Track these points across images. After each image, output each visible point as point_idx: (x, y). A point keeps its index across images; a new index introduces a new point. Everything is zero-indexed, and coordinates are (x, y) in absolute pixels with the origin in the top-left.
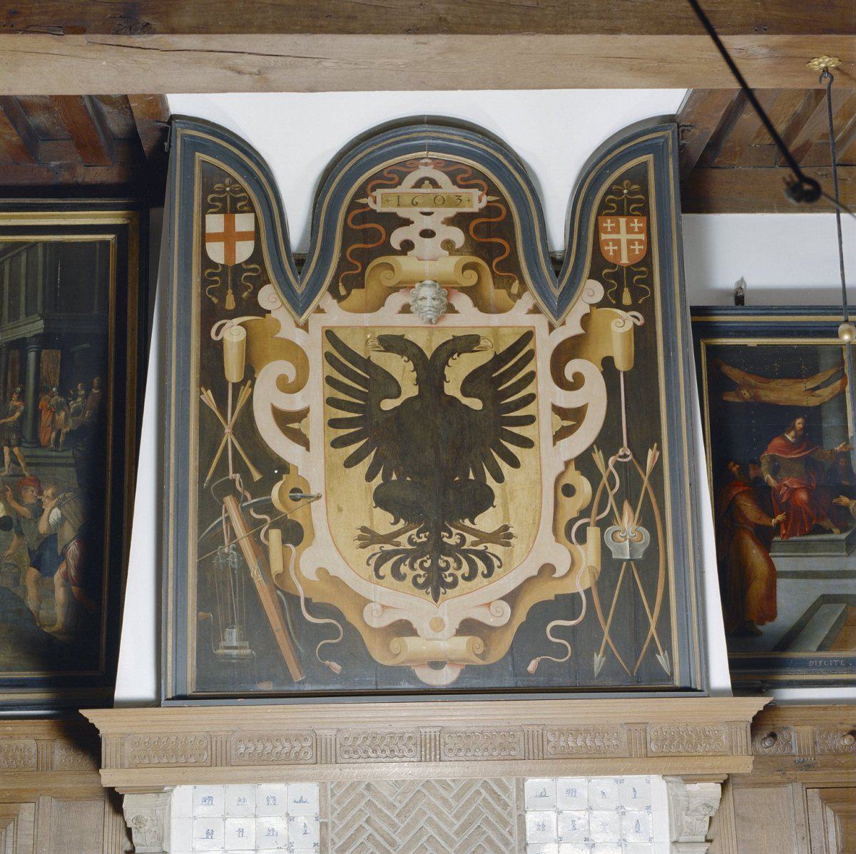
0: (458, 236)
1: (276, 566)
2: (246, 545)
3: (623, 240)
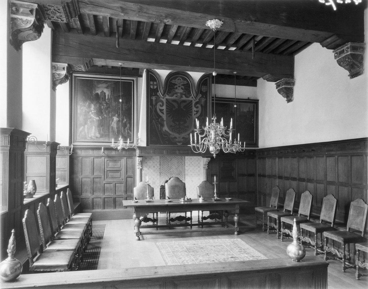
0: (183, 87)
1: (160, 129)
3: (204, 89)
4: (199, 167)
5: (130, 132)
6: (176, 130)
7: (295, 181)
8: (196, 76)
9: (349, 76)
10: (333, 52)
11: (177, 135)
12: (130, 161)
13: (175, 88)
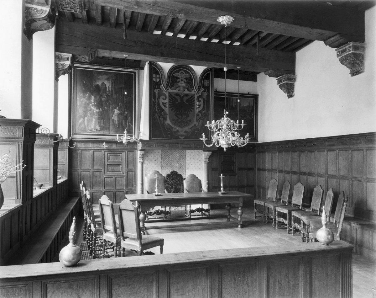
0: (186, 81)
1: (162, 123)
2: (158, 120)
3: (206, 83)
4: (200, 161)
5: (131, 125)
6: (178, 124)
7: (296, 175)
8: (199, 69)
9: (350, 74)
10: (336, 50)
11: (179, 129)
12: (131, 154)
13: (178, 81)
